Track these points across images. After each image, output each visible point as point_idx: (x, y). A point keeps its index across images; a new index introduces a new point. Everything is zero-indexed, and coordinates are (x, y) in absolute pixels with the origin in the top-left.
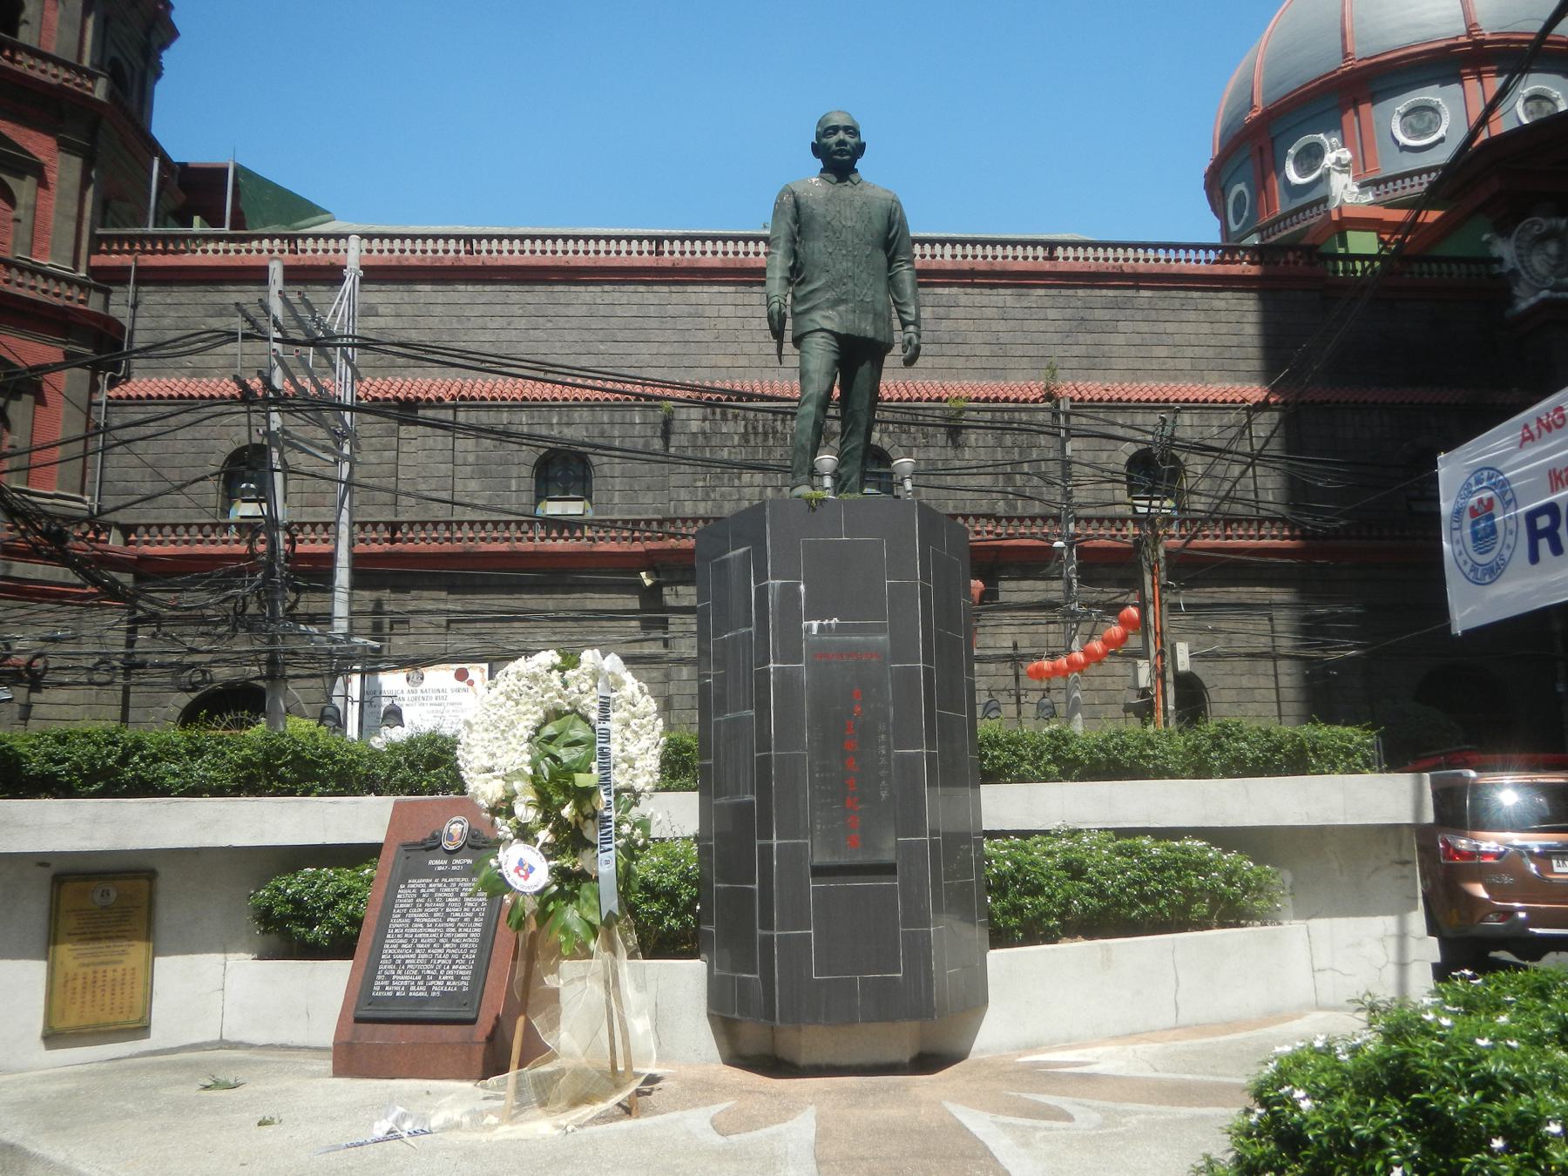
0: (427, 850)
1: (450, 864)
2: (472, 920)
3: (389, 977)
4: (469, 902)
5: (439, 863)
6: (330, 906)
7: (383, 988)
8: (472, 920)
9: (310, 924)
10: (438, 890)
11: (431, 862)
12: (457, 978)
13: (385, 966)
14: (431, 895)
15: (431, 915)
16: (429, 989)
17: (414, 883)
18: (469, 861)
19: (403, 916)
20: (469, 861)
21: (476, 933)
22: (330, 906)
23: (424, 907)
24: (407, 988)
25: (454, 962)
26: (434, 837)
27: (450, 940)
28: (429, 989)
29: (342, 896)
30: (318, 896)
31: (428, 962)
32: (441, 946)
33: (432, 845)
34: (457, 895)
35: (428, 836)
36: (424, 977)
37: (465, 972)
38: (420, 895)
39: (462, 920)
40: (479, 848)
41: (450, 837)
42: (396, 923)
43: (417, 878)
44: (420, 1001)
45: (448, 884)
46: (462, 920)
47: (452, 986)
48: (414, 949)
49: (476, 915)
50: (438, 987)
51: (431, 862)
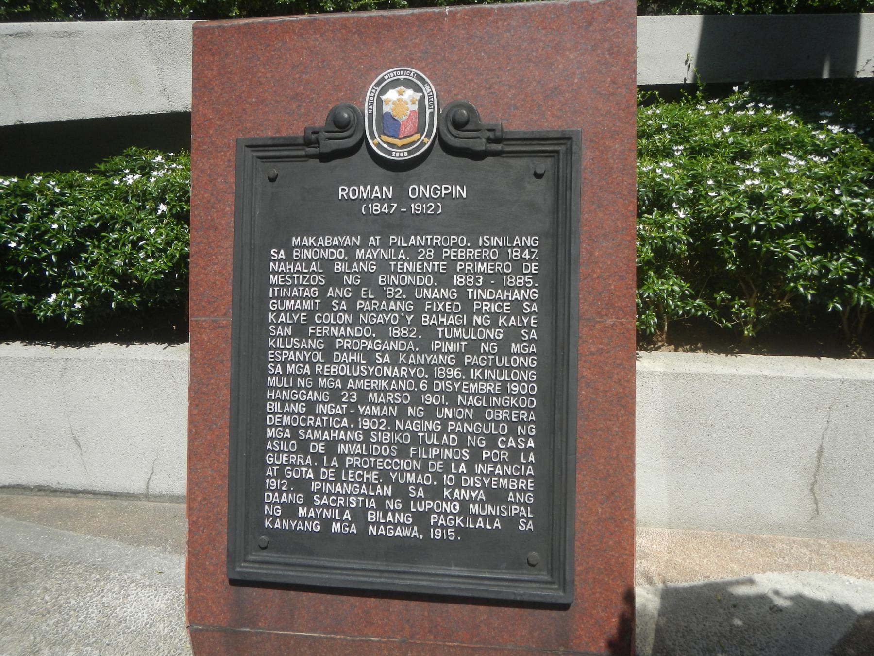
0: (325, 158)
1: (401, 196)
2: (504, 349)
3: (300, 485)
4: (486, 301)
5: (374, 195)
6: (70, 254)
7: (290, 511)
8: (504, 349)
9: (40, 287)
10: (384, 266)
11: (343, 192)
12: (496, 496)
13: (279, 455)
14: (368, 279)
15: (382, 331)
16: (422, 520)
17: (307, 246)
18: (459, 191)
19: (300, 331)
20: (459, 191)
21: (525, 381)
22: (70, 254)
23: (352, 310)
24: (359, 514)
25: (476, 455)
26: (339, 125)
27: (451, 399)
28: (422, 520)
29: (89, 232)
30: (38, 236)
31: (403, 451)
32: (430, 413)
33: (340, 143)
34: (442, 280)
35: (320, 120)
36: (401, 490)
37: (520, 485)
38: (335, 280)
39: (474, 347)
40: (478, 156)
41: (388, 124)
42: (285, 351)
43: (317, 233)
44: (401, 549)
45: (412, 253)
46: (474, 347)
47: (485, 517)
48: (354, 417)
49: (513, 334)
50: (445, 519)
51: (343, 192)
